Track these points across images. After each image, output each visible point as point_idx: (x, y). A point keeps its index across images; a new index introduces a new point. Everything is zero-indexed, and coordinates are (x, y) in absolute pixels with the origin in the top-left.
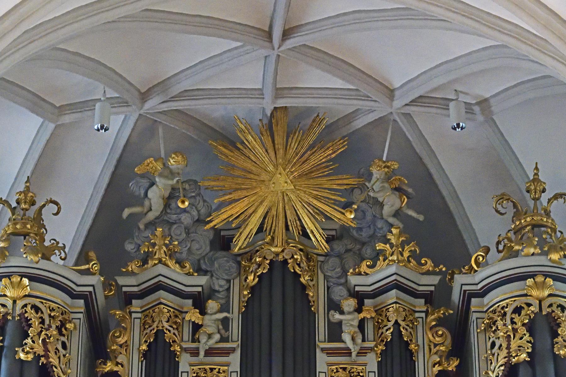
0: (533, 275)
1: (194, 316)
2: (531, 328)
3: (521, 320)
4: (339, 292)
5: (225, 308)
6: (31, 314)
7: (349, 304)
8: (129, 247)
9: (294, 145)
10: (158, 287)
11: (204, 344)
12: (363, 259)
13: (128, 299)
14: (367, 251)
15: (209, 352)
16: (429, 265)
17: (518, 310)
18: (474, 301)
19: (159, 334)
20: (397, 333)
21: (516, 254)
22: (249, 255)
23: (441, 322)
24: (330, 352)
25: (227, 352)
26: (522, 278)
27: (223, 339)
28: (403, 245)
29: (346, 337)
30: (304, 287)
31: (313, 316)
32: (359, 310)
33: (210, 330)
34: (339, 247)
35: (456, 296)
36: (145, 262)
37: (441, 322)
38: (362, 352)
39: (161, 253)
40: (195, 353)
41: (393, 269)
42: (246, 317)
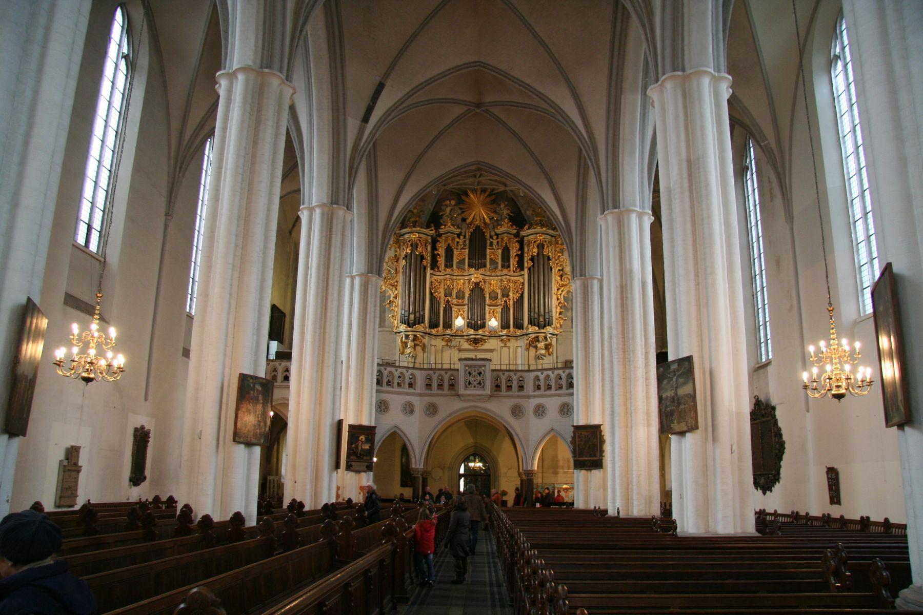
0: (539, 233)
1: (457, 240)
2: (538, 247)
3: (535, 245)
4: (493, 233)
5: (465, 237)
6: (418, 242)
7: (495, 237)
8: (441, 221)
9: (481, 198)
10: (449, 232)
11: (459, 247)
12: (498, 225)
13: (440, 235)
14: (500, 223)
15: (461, 249)
16: (515, 227)
17: (535, 242)
18: (525, 238)
19: (449, 245)
20: (506, 245)
21: (535, 228)
22: (471, 224)
23: (517, 241)
24: (490, 249)
25: (465, 249)
26: (537, 234)
27: (465, 246)
28: (508, 223)
29: (494, 247)
30: (484, 233)
31: (485, 240)
32: (497, 238)
33: (461, 243)
34: (493, 221)
35: (521, 236)
36: (445, 226)
37: (517, 241)
38: (498, 249)
39: (449, 224)
40: (457, 249)
41: (506, 229)
42: (470, 240)
